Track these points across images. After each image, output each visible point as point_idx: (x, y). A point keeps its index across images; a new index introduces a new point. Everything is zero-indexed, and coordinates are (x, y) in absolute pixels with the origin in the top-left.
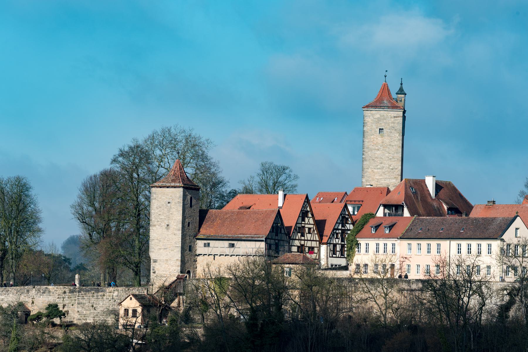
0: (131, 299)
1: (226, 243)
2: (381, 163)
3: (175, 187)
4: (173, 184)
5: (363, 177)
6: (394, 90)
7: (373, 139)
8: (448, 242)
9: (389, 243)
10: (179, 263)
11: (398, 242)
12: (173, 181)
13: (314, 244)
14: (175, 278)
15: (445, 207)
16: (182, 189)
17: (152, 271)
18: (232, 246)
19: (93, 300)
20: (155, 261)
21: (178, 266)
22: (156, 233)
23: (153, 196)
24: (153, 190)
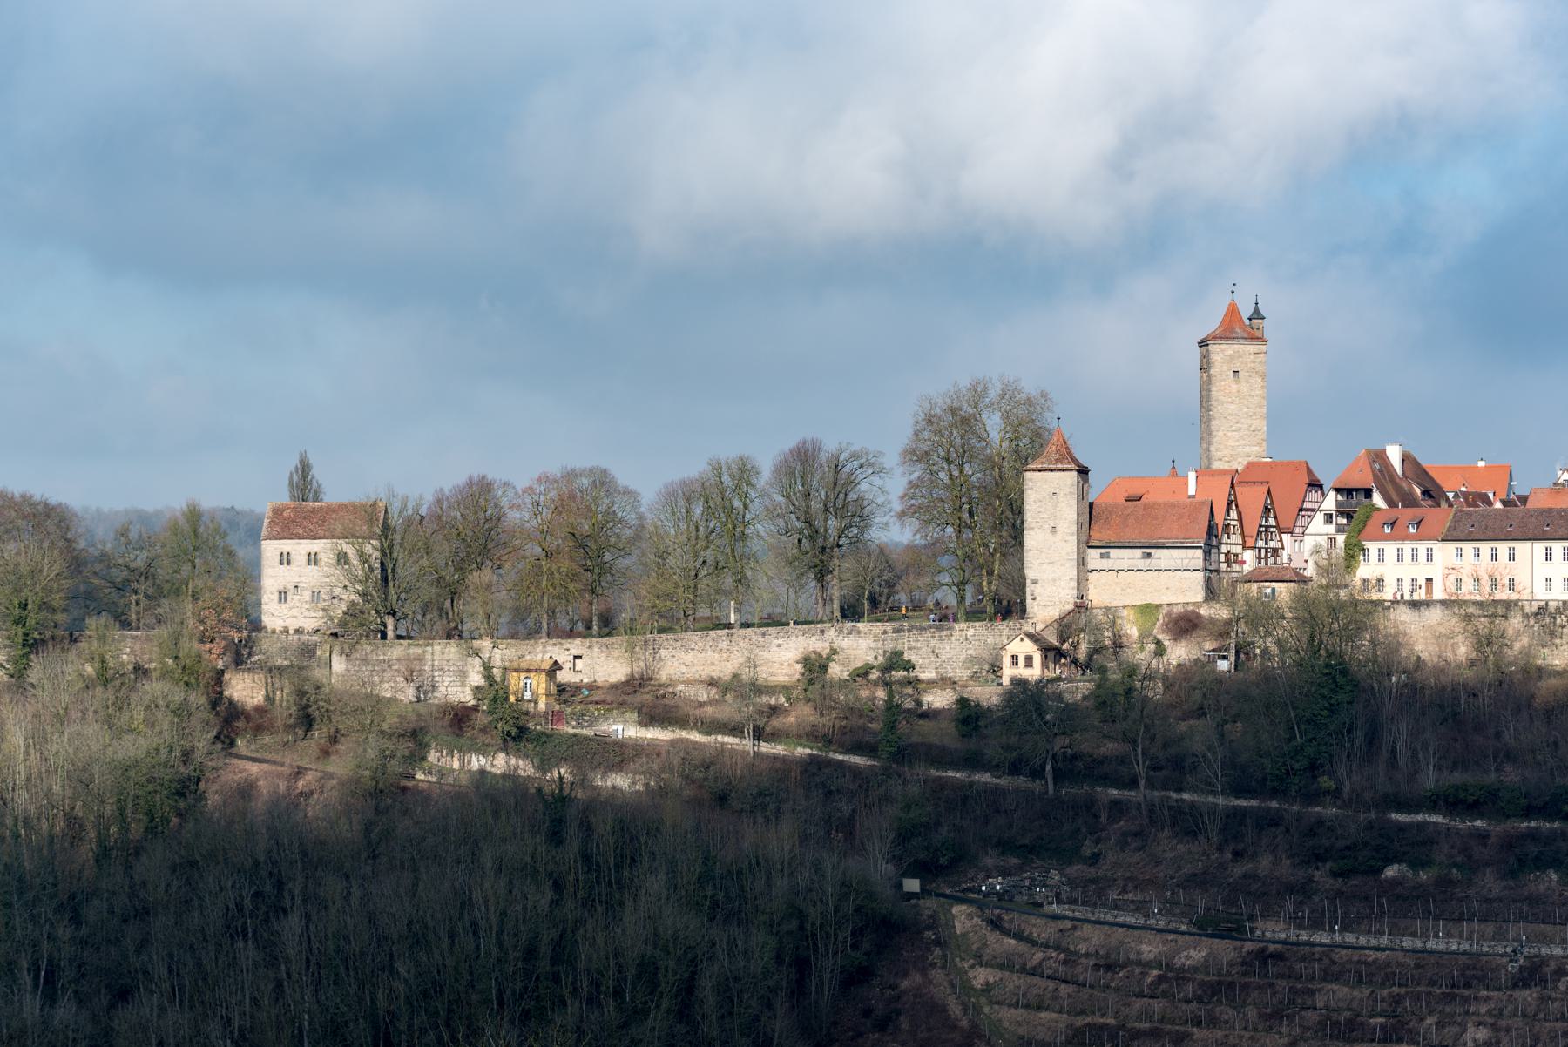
1: (1138, 552)
5: (1209, 443)
6: (1246, 311)
7: (1223, 388)
8: (1528, 544)
9: (1422, 547)
11: (1439, 548)
12: (1057, 461)
13: (1237, 549)
14: (1070, 607)
15: (1418, 491)
17: (1029, 598)
18: (1149, 555)
19: (933, 643)
20: (1035, 582)
22: (1032, 539)
23: (1028, 485)
24: (1028, 475)
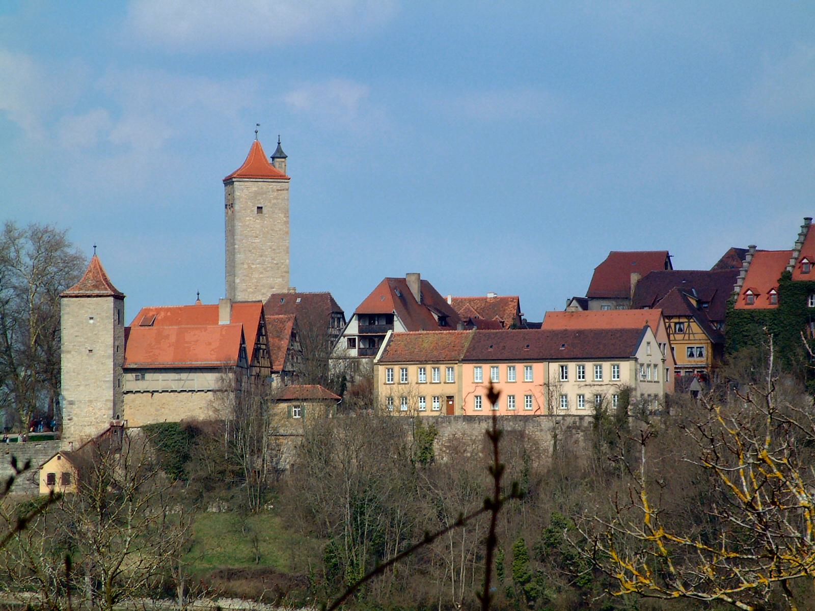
0: (59, 458)
2: (261, 256)
3: (100, 296)
4: (96, 292)
10: (111, 405)
12: (96, 287)
16: (112, 299)
20: (71, 403)
21: (109, 409)
